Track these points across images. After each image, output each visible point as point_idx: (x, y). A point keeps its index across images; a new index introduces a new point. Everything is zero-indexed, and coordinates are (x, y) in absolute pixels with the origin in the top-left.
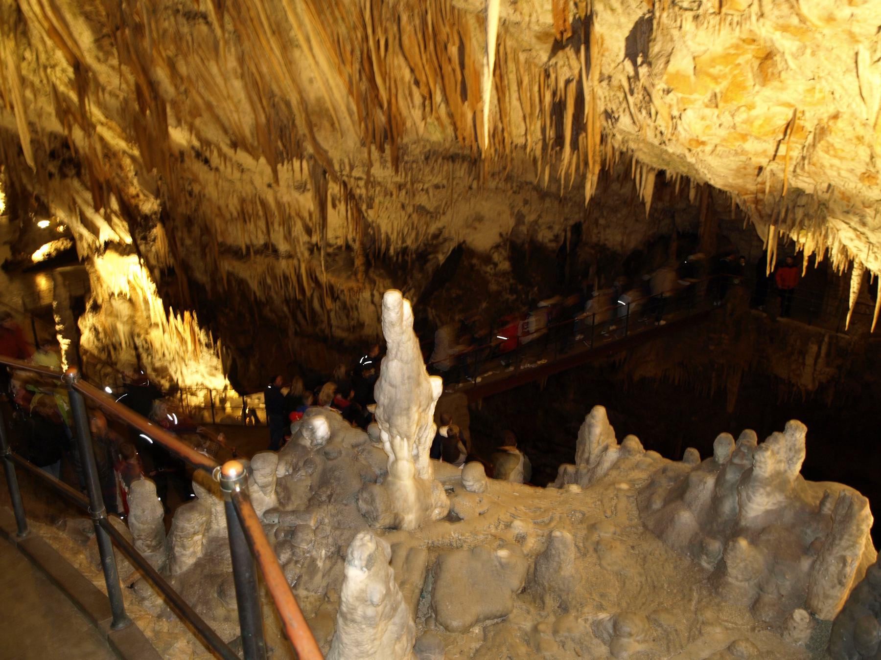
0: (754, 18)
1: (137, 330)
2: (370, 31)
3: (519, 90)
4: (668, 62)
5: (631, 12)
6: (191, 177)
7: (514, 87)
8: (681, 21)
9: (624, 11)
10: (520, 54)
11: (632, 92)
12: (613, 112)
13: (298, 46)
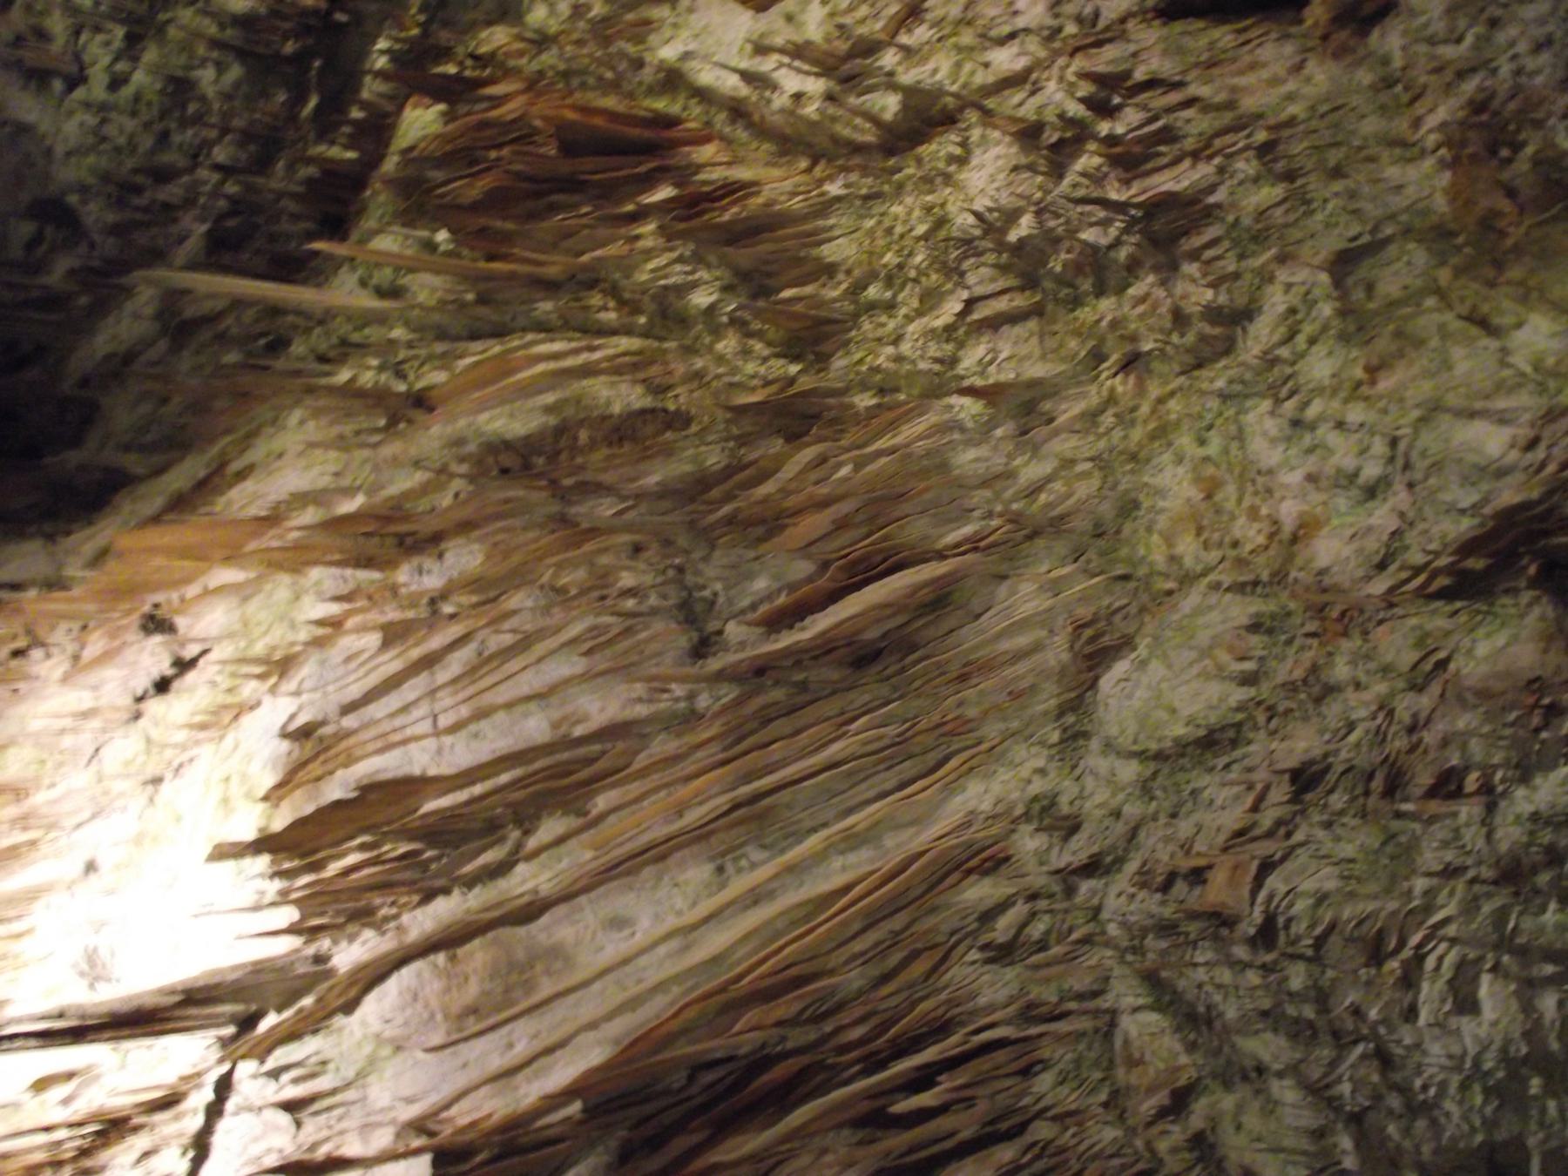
6: (89, 653)
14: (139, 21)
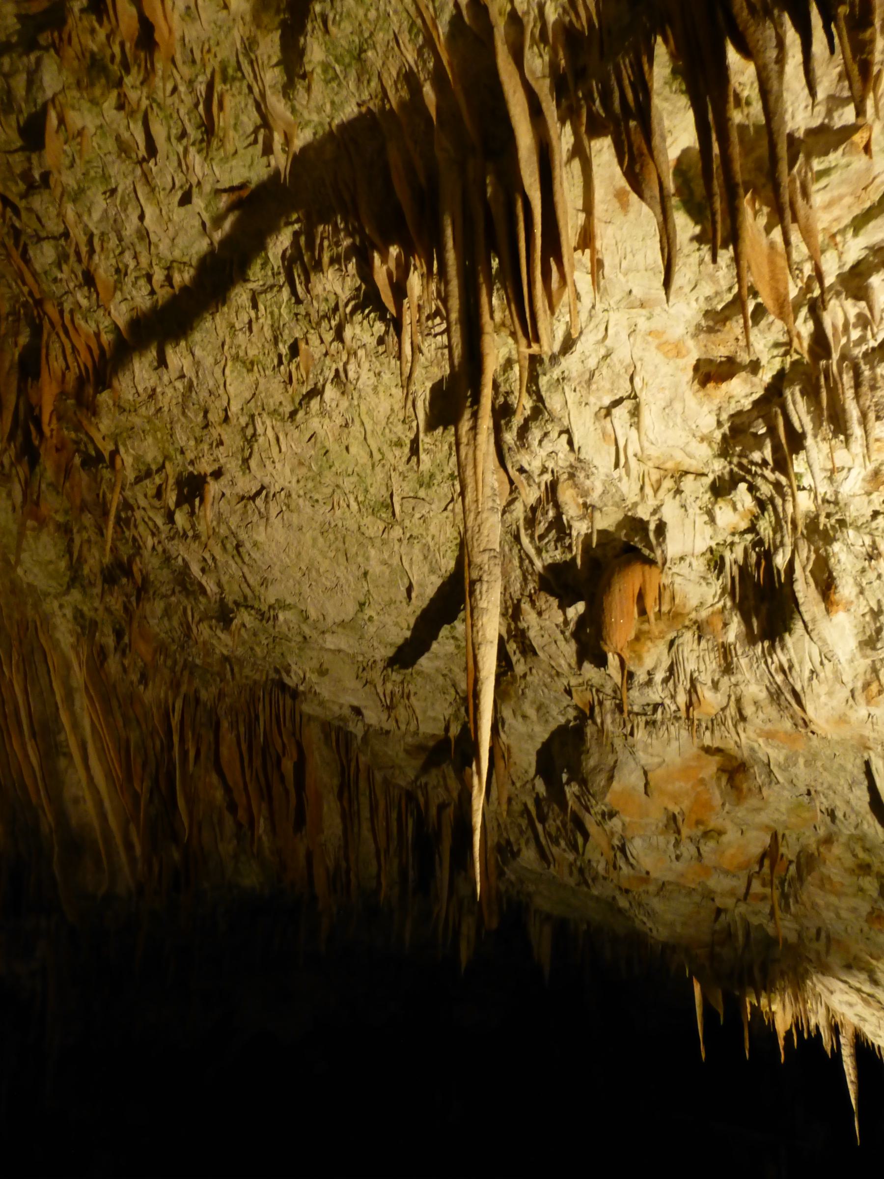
0: (729, 722)
2: (176, 739)
3: (372, 820)
4: (611, 779)
5: (550, 719)
7: (365, 813)
8: (632, 728)
9: (539, 718)
10: (376, 772)
11: (543, 819)
12: (508, 842)
13: (69, 756)
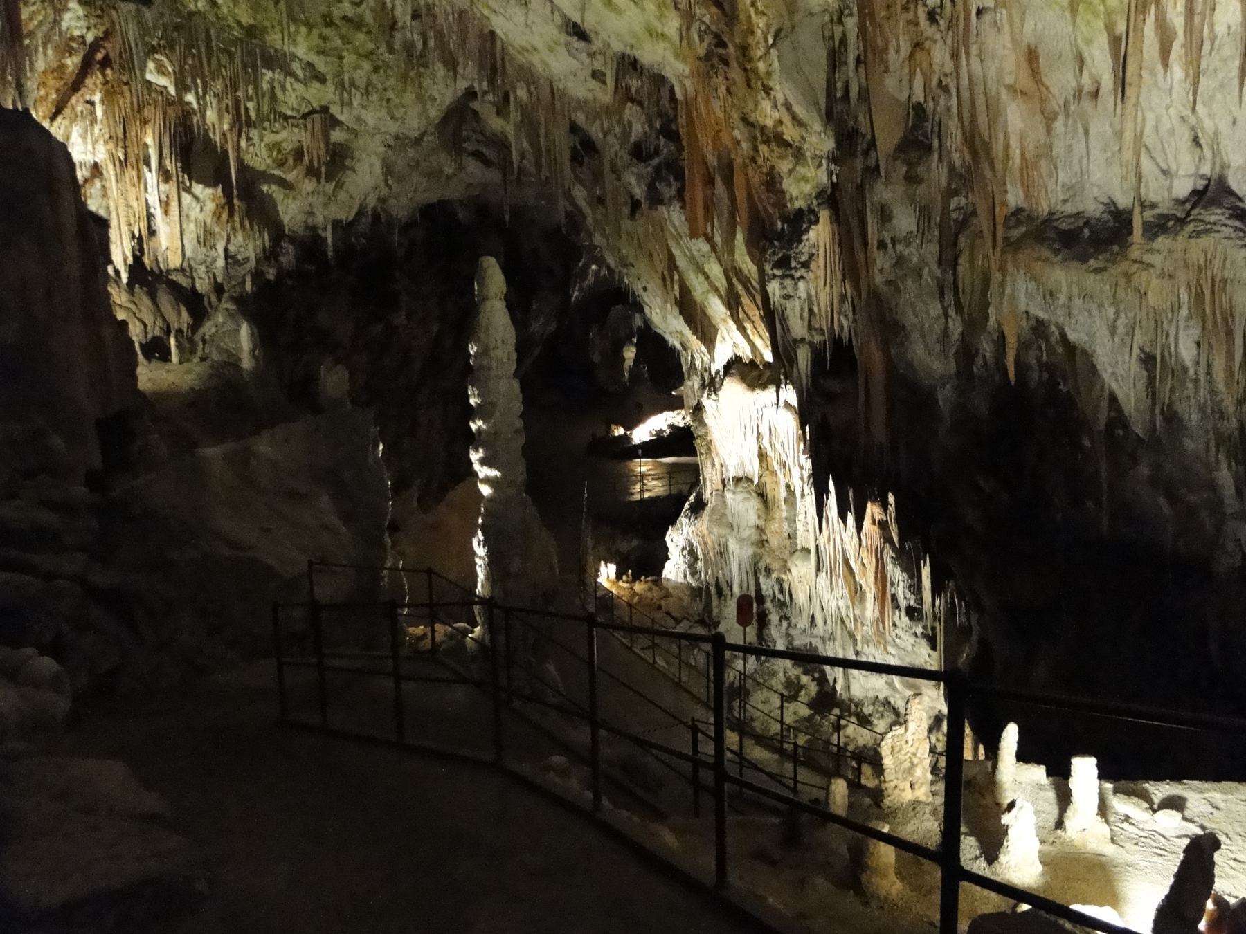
1: (766, 561)
14: (250, 53)
